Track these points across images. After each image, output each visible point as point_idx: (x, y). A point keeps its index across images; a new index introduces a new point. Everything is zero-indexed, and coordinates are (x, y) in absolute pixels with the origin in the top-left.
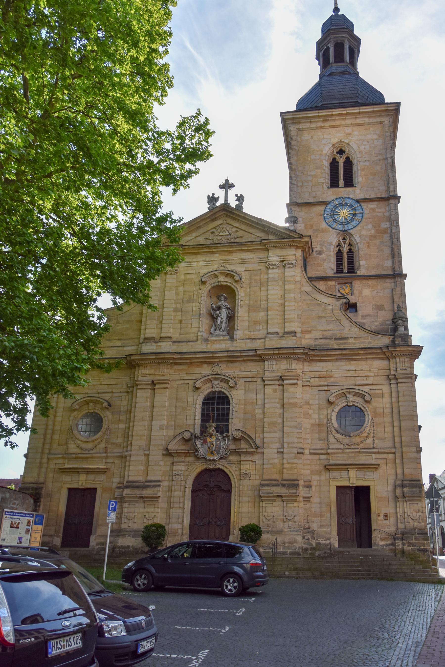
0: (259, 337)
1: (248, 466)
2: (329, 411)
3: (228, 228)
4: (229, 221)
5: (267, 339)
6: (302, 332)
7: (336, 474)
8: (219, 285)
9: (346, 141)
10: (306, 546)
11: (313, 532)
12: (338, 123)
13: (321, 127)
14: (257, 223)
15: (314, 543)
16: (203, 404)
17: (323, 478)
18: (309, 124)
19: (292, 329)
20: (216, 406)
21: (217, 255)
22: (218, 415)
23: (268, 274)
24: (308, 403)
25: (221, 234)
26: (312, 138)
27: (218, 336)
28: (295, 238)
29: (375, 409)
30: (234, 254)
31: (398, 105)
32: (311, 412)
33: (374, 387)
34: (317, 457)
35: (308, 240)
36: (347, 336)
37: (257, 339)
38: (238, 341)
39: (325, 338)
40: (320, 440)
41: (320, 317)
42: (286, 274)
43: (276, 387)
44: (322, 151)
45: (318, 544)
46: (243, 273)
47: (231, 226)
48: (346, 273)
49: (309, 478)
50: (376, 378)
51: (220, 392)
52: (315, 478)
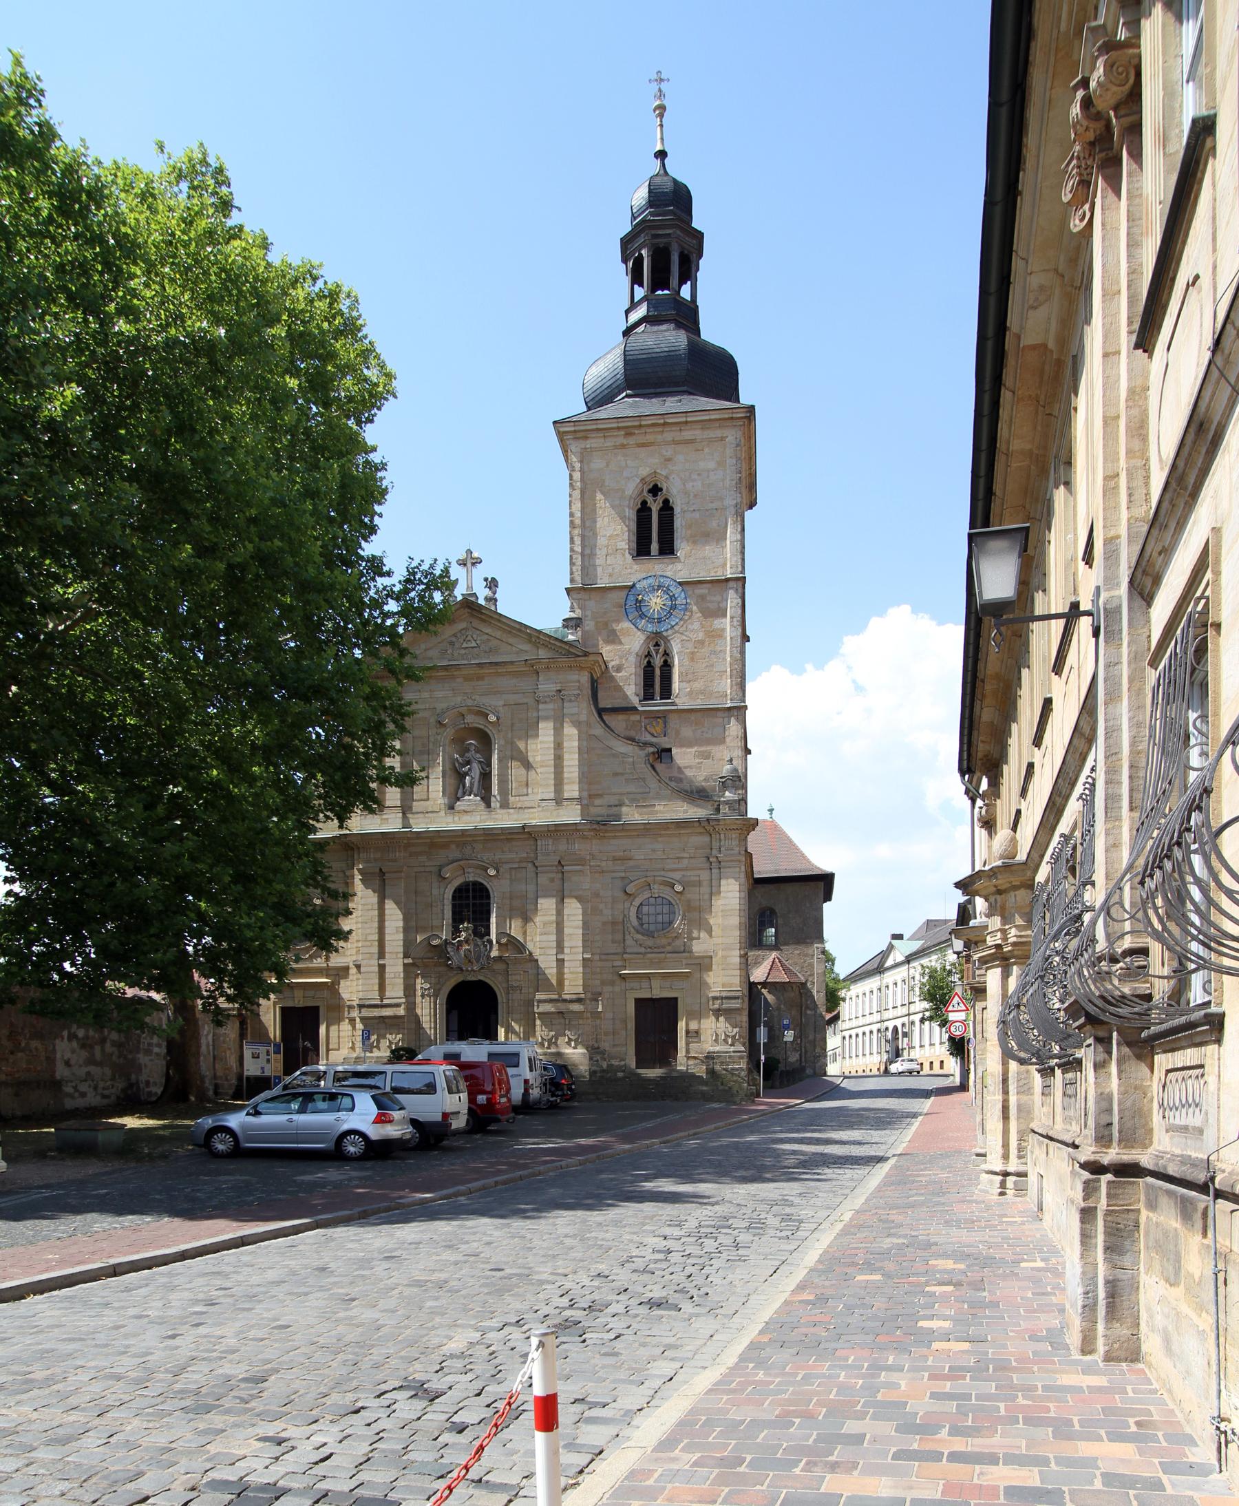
1: (517, 977)
2: (627, 905)
4: (476, 623)
7: (635, 985)
9: (664, 473)
10: (594, 1068)
11: (603, 1053)
12: (650, 438)
13: (623, 446)
14: (520, 630)
15: (605, 1065)
16: (454, 898)
17: (617, 989)
20: (471, 901)
22: (474, 912)
23: (538, 710)
24: (597, 895)
25: (465, 645)
26: (607, 465)
29: (689, 901)
31: (753, 407)
32: (601, 906)
33: (688, 873)
34: (609, 964)
40: (613, 942)
41: (616, 774)
42: (565, 711)
43: (552, 875)
44: (623, 491)
45: (610, 1066)
49: (599, 990)
50: (692, 861)
51: (475, 884)
52: (607, 989)
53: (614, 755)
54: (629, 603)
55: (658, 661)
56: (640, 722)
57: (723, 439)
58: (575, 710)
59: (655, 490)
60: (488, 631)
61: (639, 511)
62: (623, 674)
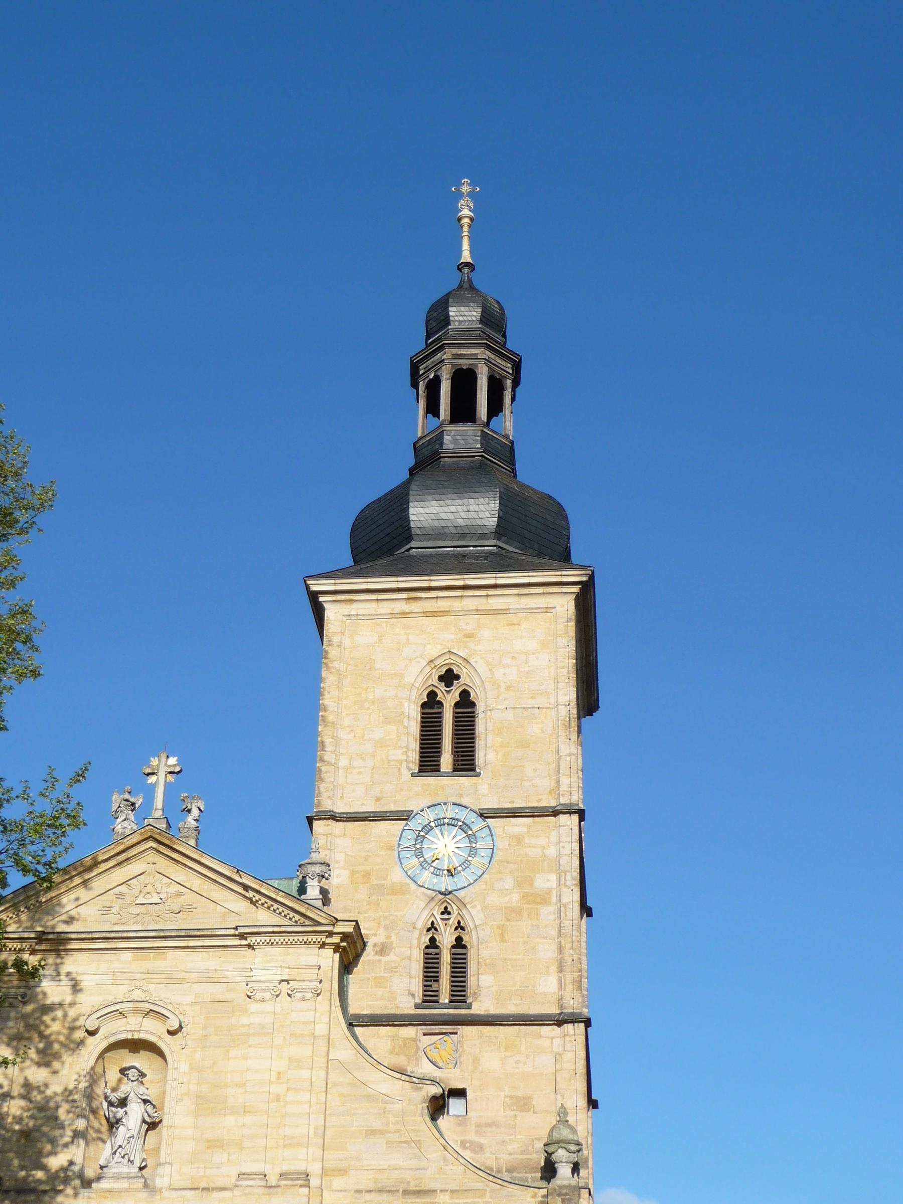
0: (219, 1184)
3: (158, 885)
4: (163, 864)
5: (237, 1192)
6: (324, 1172)
8: (126, 1040)
12: (443, 605)
13: (404, 615)
18: (374, 605)
19: (300, 1166)
21: (127, 956)
26: (380, 641)
27: (118, 1177)
28: (320, 924)
30: (170, 954)
35: (349, 928)
36: (432, 1186)
37: (213, 1189)
38: (166, 1193)
39: (380, 1191)
41: (371, 1132)
46: (188, 1008)
47: (166, 880)
48: (445, 1006)
53: (369, 1098)
54: (405, 843)
55: (446, 939)
56: (415, 1040)
57: (547, 610)
58: (309, 1016)
59: (449, 678)
60: (180, 874)
61: (424, 706)
62: (391, 957)
